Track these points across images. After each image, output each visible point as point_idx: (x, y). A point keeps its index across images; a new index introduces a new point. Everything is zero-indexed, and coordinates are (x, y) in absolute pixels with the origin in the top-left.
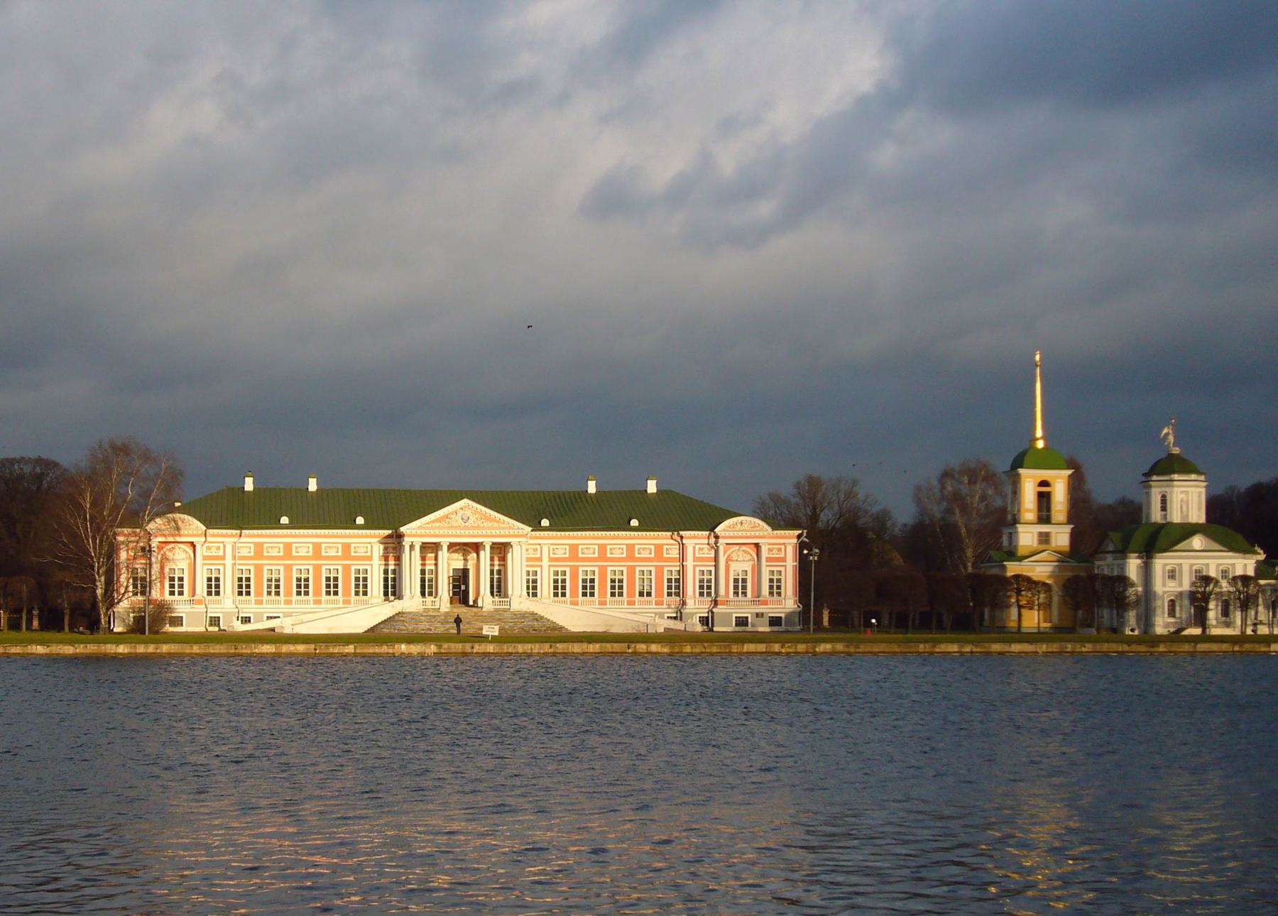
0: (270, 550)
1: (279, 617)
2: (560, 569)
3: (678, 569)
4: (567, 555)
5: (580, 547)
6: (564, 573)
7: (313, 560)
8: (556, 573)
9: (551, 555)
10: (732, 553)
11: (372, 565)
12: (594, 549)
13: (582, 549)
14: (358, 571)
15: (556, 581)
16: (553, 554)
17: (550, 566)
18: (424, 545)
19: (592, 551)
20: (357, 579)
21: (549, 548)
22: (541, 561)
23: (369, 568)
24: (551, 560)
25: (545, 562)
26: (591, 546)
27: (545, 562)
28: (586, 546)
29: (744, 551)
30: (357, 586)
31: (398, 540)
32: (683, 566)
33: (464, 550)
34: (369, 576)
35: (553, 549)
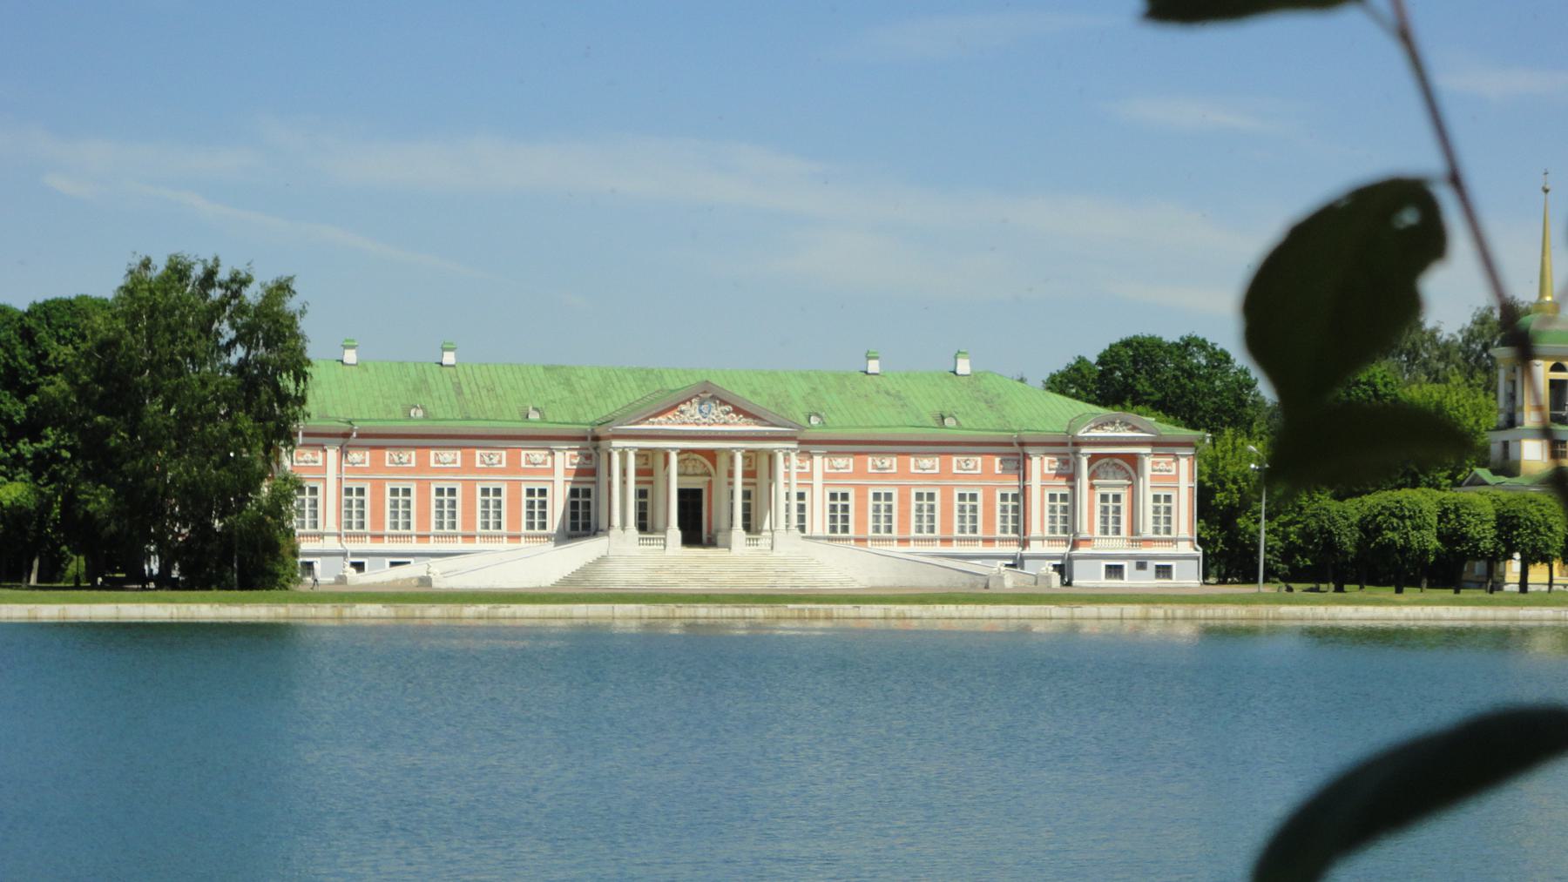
0: (487, 459)
1: (409, 563)
2: (839, 491)
3: (1016, 491)
4: (851, 470)
7: (464, 473)
8: (833, 496)
9: (827, 470)
10: (1098, 467)
11: (553, 481)
14: (530, 492)
15: (833, 508)
17: (824, 485)
18: (640, 453)
20: (531, 504)
23: (549, 487)
25: (818, 481)
27: (818, 481)
29: (1115, 464)
30: (531, 515)
31: (595, 443)
32: (1024, 487)
33: (695, 460)
34: (548, 498)
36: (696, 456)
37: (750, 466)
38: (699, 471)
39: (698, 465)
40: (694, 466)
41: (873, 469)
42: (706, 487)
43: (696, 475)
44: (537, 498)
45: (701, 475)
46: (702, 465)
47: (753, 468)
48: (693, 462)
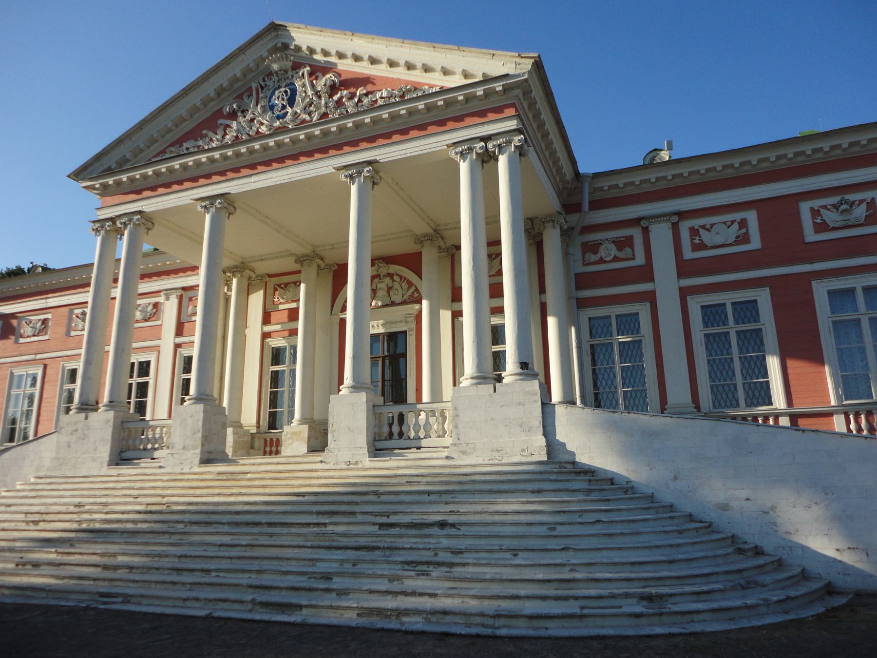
5: (805, 207)
8: (713, 314)
9: (688, 254)
13: (815, 213)
16: (695, 248)
17: (684, 293)
19: (860, 212)
21: (675, 227)
22: (652, 279)
23: (152, 357)
24: (684, 268)
26: (851, 197)
28: (835, 200)
33: (390, 276)
35: (694, 232)
36: (394, 268)
38: (397, 298)
40: (389, 289)
41: (817, 231)
43: (393, 304)
45: (404, 303)
48: (388, 280)
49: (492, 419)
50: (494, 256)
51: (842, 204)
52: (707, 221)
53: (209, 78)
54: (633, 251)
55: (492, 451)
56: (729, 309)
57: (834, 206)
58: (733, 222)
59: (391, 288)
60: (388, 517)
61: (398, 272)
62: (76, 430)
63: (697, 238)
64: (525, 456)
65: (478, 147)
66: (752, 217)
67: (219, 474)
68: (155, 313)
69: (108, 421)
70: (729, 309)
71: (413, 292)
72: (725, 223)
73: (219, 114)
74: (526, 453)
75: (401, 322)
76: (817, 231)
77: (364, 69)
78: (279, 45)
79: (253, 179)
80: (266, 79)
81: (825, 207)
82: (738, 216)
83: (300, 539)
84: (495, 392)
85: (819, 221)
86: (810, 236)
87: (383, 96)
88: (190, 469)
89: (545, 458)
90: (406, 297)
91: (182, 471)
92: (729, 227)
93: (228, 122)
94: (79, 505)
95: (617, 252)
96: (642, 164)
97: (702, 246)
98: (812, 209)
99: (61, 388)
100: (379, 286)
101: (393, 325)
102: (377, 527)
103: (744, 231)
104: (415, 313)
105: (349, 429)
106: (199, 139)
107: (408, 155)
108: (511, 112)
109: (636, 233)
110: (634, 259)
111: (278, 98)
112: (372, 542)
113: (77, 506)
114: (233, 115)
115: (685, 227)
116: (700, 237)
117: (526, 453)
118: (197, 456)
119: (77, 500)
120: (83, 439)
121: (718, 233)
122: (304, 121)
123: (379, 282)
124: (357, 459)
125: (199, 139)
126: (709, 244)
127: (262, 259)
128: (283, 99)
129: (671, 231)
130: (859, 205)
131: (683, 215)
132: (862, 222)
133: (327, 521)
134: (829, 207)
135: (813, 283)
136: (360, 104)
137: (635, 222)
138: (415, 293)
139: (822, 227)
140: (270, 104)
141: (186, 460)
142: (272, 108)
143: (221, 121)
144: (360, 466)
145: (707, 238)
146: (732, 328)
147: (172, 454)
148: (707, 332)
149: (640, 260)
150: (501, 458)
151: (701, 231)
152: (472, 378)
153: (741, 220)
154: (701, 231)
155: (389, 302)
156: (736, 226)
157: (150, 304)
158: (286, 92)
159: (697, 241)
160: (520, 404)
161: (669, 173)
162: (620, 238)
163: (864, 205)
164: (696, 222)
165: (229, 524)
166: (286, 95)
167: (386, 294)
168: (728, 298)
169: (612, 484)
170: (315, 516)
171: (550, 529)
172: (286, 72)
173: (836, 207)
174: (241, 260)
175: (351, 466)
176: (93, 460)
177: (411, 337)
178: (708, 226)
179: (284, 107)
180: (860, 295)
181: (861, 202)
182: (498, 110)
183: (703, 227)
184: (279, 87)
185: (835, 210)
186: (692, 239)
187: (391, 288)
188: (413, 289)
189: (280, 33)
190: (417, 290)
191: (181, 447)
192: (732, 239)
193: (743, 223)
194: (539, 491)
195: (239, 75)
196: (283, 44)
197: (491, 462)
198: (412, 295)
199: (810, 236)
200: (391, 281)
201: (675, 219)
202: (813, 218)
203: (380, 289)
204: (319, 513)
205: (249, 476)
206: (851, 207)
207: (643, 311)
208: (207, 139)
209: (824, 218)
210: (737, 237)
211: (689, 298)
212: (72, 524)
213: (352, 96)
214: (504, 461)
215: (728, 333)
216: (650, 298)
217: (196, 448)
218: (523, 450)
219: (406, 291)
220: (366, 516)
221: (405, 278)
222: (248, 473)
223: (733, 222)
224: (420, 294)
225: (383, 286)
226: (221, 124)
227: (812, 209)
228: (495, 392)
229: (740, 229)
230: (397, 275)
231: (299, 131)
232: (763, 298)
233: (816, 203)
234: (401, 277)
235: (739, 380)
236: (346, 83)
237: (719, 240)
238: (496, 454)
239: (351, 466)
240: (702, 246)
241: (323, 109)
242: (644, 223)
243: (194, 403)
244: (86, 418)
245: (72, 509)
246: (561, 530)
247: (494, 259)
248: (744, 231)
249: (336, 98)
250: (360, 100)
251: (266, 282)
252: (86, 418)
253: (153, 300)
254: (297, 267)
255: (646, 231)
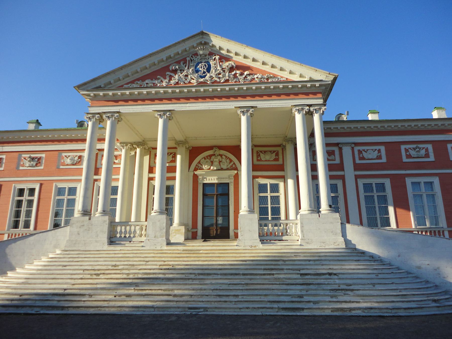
4: (384, 160)
5: (403, 147)
6: (381, 187)
8: (368, 187)
9: (358, 161)
12: (427, 150)
13: (407, 150)
14: (60, 191)
15: (369, 199)
17: (357, 177)
19: (423, 152)
20: (59, 203)
21: (353, 148)
22: (343, 170)
24: (357, 167)
26: (421, 146)
28: (414, 146)
33: (221, 155)
35: (360, 152)
36: (222, 152)
37: (276, 160)
38: (225, 167)
39: (224, 160)
40: (220, 162)
41: (407, 158)
42: (233, 181)
43: (222, 169)
44: (66, 197)
45: (227, 169)
46: (228, 160)
47: (280, 162)
48: (219, 157)
49: (319, 229)
50: (272, 152)
51: (416, 148)
52: (366, 148)
53: (164, 51)
54: (335, 157)
55: (321, 243)
56: (374, 186)
57: (414, 148)
58: (376, 150)
59: (221, 161)
60: (300, 271)
61: (225, 154)
62: (83, 226)
63: (361, 155)
64: (336, 245)
65: (306, 109)
66: (383, 148)
67: (183, 250)
68: (79, 162)
69: (105, 221)
70: (374, 186)
71: (232, 165)
72: (372, 150)
73: (167, 68)
74: (336, 244)
75: (226, 178)
76: (407, 158)
77: (248, 62)
78: (203, 42)
79: (188, 105)
80: (193, 57)
81: (410, 148)
82: (377, 147)
83: (266, 281)
84: (319, 217)
85: (408, 154)
86: (405, 160)
87: (259, 77)
88: (161, 248)
89: (344, 247)
90: (229, 166)
91: (156, 249)
92: (374, 152)
93: (172, 74)
94: (115, 266)
95: (328, 157)
96: (335, 120)
97: (363, 158)
98: (405, 149)
99: (13, 199)
100: (215, 160)
101: (222, 180)
102: (299, 275)
103: (380, 154)
104: (234, 174)
105: (249, 230)
106: (154, 80)
107: (272, 107)
108: (320, 96)
109: (336, 149)
110: (335, 160)
111: (201, 67)
112: (303, 281)
113: (113, 266)
114: (175, 71)
115: (356, 149)
116: (362, 154)
117: (336, 244)
118: (164, 241)
119: (114, 263)
120: (88, 230)
121: (370, 154)
122: (215, 82)
123: (215, 158)
124: (255, 244)
125: (154, 80)
126: (366, 158)
127: (155, 140)
128: (204, 69)
129: (351, 150)
130: (422, 149)
131: (356, 144)
132: (423, 156)
133: (275, 273)
134: (412, 149)
135: (406, 178)
136: (246, 79)
137: (337, 144)
138: (234, 165)
139: (409, 156)
140: (196, 69)
141: (158, 243)
142: (197, 71)
143: (167, 73)
144: (257, 248)
145: (365, 155)
146: (375, 194)
147: (149, 240)
148: (366, 195)
149: (338, 161)
150: (325, 246)
151: (363, 152)
152: (308, 210)
153: (379, 149)
154: (363, 152)
155: (220, 168)
156: (377, 152)
157: (76, 156)
158: (205, 65)
159: (361, 156)
160: (331, 223)
161: (346, 126)
162: (329, 150)
163: (424, 149)
164: (361, 148)
165: (221, 274)
166: (206, 67)
167: (218, 164)
168: (374, 181)
169: (373, 258)
170: (262, 271)
171: (376, 276)
172: (206, 56)
173: (414, 149)
174: (143, 139)
175: (253, 248)
176: (96, 242)
177: (232, 186)
178: (366, 150)
179: (204, 72)
180: (422, 185)
181: (423, 148)
182: (315, 94)
183: (364, 150)
184: (201, 62)
185: (414, 150)
186: (359, 155)
187: (221, 161)
188: (232, 163)
189: (204, 36)
190: (234, 164)
191: (153, 236)
192: (375, 157)
193: (379, 151)
194: (358, 260)
195: (180, 52)
196: (205, 42)
197: (321, 247)
198: (232, 166)
199: (405, 160)
200: (221, 158)
201: (353, 145)
202: (406, 152)
203: (215, 161)
204: (265, 269)
205: (201, 252)
206: (420, 150)
207: (339, 183)
208: (159, 81)
209: (410, 153)
210: (377, 156)
211: (358, 179)
212: (123, 275)
213: (241, 74)
214: (327, 247)
215: (374, 196)
216: (343, 178)
217: (163, 237)
218: (335, 243)
219: (229, 164)
220: (288, 271)
221: (228, 158)
222: (201, 250)
223: (376, 150)
224: (236, 166)
225: (217, 160)
226: (168, 75)
227: (405, 149)
228: (319, 217)
229: (378, 153)
230: (224, 155)
231: (217, 87)
232: (387, 183)
233: (407, 146)
234: (226, 157)
235: (378, 216)
236: (238, 67)
237: (370, 157)
238: (322, 244)
239: (253, 248)
240: (363, 158)
241: (227, 78)
242: (340, 146)
243: (159, 214)
244: (90, 219)
245: (110, 267)
246: (380, 276)
247: (273, 153)
248: (380, 154)
249: (233, 73)
250: (246, 77)
251: (150, 152)
252: (90, 219)
253: (79, 154)
254: (174, 146)
255: (340, 149)
